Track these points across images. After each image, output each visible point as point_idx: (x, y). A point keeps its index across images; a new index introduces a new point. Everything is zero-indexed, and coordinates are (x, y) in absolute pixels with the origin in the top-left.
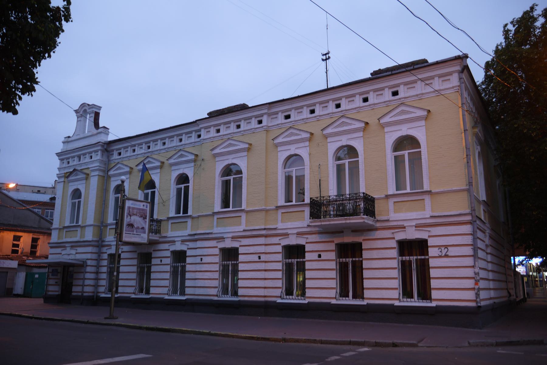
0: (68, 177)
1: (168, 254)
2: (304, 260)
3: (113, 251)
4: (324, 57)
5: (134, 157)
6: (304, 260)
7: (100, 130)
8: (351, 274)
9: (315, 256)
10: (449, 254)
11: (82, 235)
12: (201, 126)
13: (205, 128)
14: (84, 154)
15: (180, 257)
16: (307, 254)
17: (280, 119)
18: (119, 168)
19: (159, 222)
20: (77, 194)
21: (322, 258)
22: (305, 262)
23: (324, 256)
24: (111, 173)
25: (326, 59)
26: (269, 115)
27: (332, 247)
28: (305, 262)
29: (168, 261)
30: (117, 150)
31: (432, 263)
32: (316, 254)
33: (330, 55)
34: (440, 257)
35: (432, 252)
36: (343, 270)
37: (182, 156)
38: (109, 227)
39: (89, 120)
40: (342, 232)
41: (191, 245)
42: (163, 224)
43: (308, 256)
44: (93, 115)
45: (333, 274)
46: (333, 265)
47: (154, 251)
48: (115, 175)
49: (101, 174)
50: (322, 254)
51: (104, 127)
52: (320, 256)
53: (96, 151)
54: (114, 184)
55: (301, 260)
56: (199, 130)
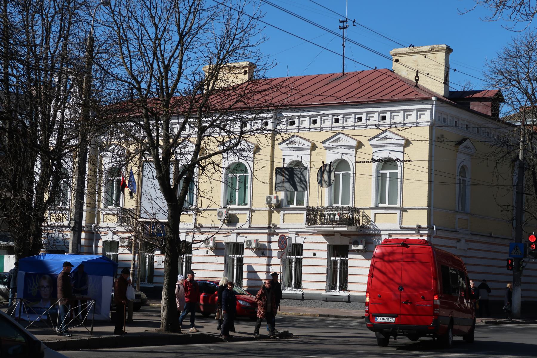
2: (301, 257)
3: (109, 237)
6: (301, 257)
9: (310, 254)
16: (304, 252)
22: (302, 259)
23: (318, 254)
28: (302, 259)
32: (312, 252)
36: (332, 266)
40: (333, 235)
45: (324, 270)
46: (325, 262)
50: (317, 252)
52: (314, 254)
55: (299, 257)
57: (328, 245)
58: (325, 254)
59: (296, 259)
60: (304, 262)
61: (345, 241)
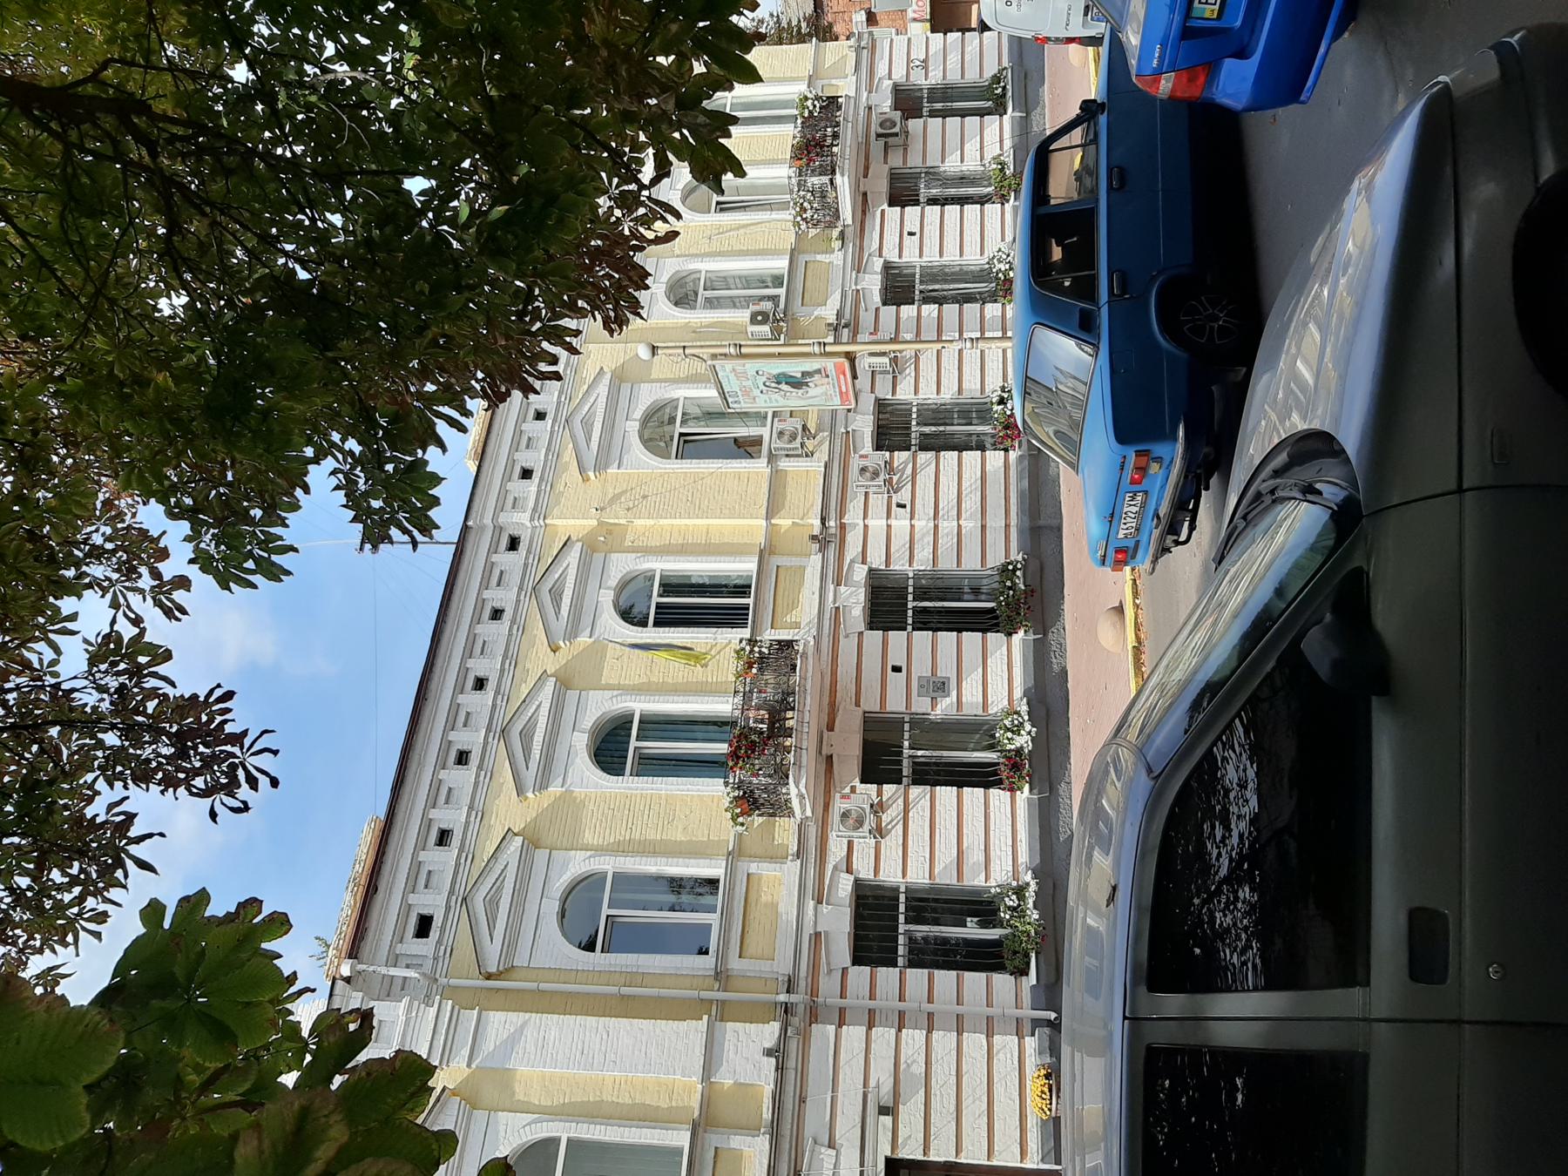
5: (474, 827)
10: (922, 57)
12: (488, 521)
13: (500, 508)
15: (888, 604)
21: (917, 230)
31: (935, 78)
34: (926, 68)
35: (918, 79)
37: (556, 595)
38: (735, 964)
40: (865, 194)
41: (853, 549)
43: (911, 256)
47: (858, 704)
48: (510, 944)
56: (499, 529)
57: (890, 205)
59: (921, 282)
60: (931, 257)
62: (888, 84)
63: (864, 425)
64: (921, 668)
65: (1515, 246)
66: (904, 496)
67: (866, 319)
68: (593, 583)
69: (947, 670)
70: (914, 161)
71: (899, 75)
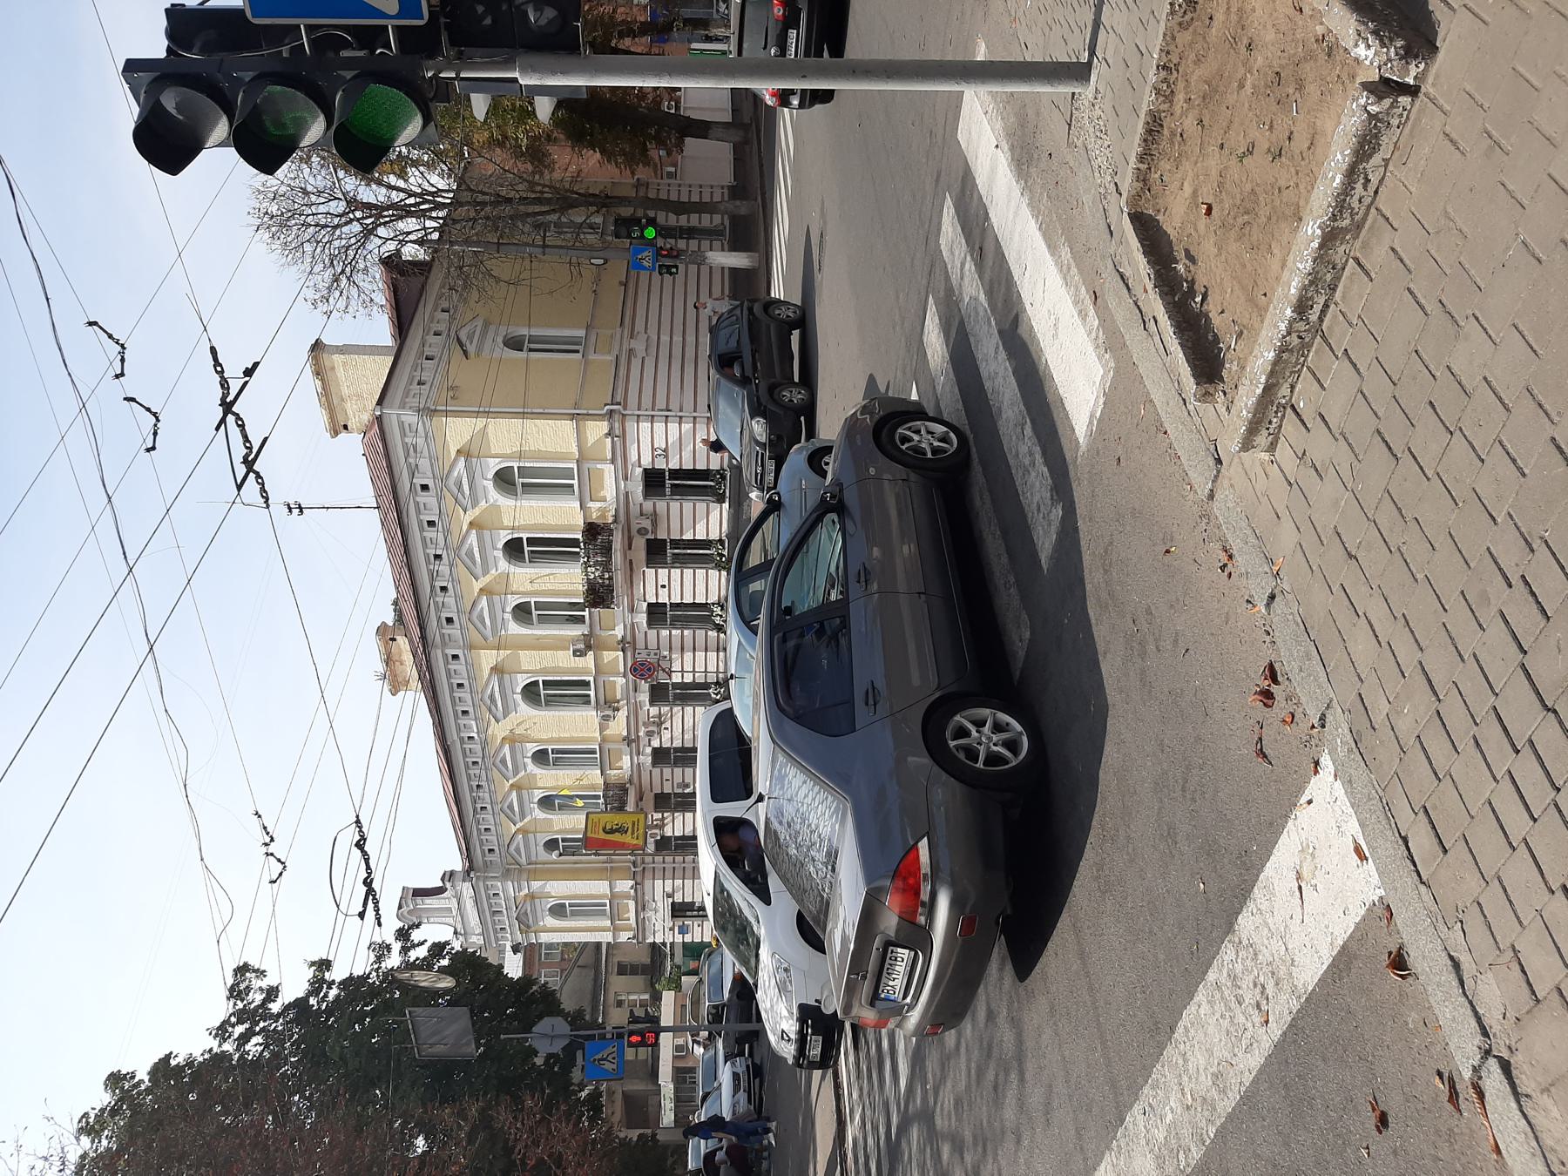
0: (528, 927)
1: (656, 771)
4: (296, 511)
7: (448, 885)
8: (692, 553)
11: (628, 897)
13: (459, 730)
14: (490, 906)
15: (660, 756)
17: (453, 631)
18: (518, 850)
19: (607, 786)
20: (558, 911)
24: (523, 860)
25: (301, 509)
26: (444, 645)
27: (650, 572)
29: (667, 771)
30: (484, 855)
31: (674, 465)
33: (292, 503)
34: (666, 457)
35: (661, 464)
36: (682, 561)
39: (431, 902)
42: (612, 780)
43: (663, 599)
44: (419, 900)
45: (688, 573)
46: (676, 573)
48: (528, 856)
49: (525, 876)
51: (443, 879)
53: (487, 888)
54: (543, 855)
58: (663, 572)
61: (640, 543)
62: (639, 471)
63: (644, 697)
64: (678, 780)
65: (1067, 414)
66: (668, 725)
67: (640, 637)
68: (519, 756)
69: (688, 780)
70: (662, 535)
71: (646, 462)
